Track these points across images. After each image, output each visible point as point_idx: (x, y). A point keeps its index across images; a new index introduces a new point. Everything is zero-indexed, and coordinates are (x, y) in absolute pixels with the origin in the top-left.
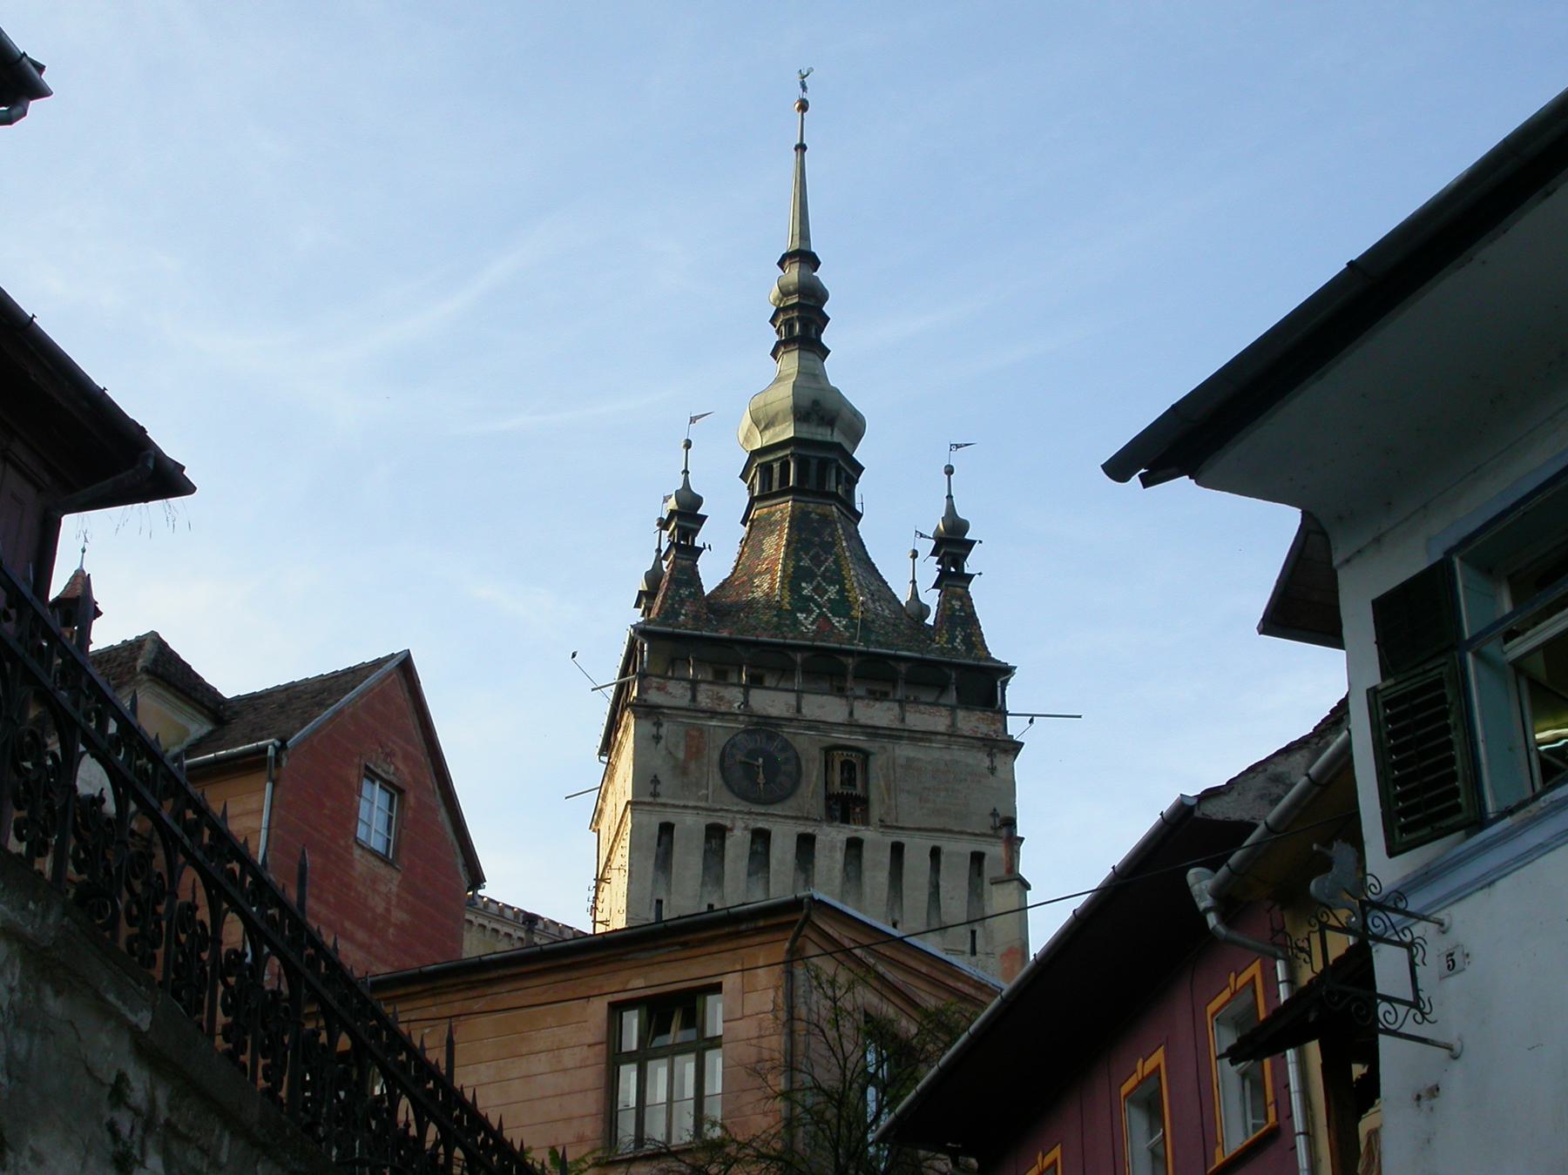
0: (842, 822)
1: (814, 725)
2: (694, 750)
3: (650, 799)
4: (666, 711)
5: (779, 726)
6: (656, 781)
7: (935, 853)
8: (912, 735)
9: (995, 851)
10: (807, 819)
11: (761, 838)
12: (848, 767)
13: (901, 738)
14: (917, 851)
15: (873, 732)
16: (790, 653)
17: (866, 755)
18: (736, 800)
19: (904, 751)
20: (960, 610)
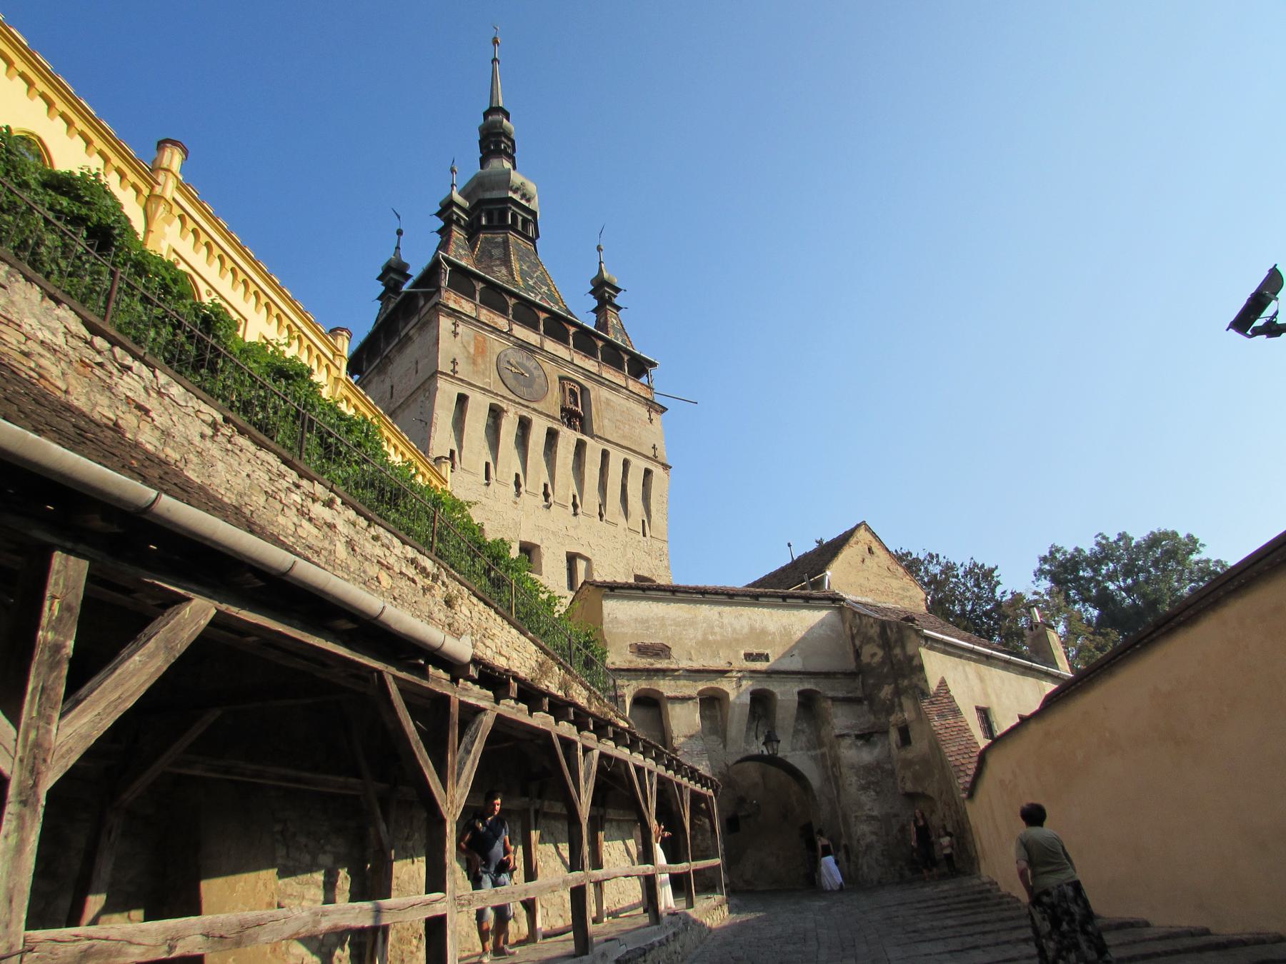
1: (554, 358)
3: (452, 374)
5: (534, 352)
6: (454, 362)
7: (626, 463)
8: (610, 384)
9: (657, 471)
10: (554, 418)
11: (524, 425)
12: (572, 393)
13: (603, 384)
14: (616, 458)
15: (588, 374)
16: (536, 311)
17: (583, 389)
18: (508, 391)
19: (604, 393)
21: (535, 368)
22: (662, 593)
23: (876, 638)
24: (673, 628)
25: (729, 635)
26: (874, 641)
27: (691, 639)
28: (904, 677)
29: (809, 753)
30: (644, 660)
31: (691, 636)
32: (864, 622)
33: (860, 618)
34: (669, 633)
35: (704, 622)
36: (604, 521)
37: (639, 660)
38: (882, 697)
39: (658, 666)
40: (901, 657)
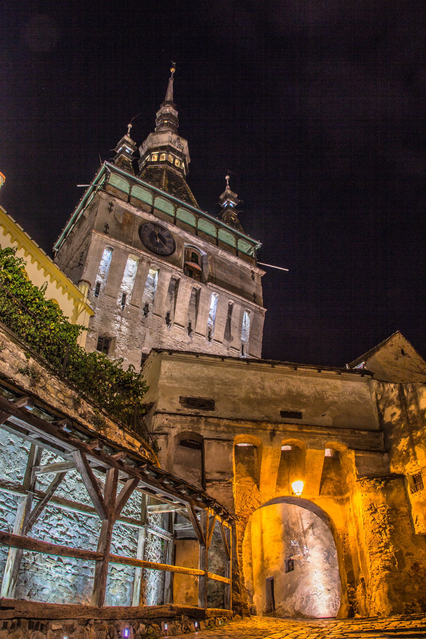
0: (189, 277)
2: (127, 221)
4: (117, 199)
6: (107, 226)
20: (235, 220)
21: (167, 236)
22: (213, 359)
23: (396, 400)
24: (220, 386)
25: (269, 395)
26: (394, 403)
27: (235, 396)
28: (418, 429)
29: (336, 497)
30: (190, 410)
31: (235, 394)
32: (387, 389)
33: (383, 386)
34: (216, 390)
35: (247, 384)
36: (212, 340)
37: (186, 409)
38: (400, 450)
39: (204, 415)
40: (415, 412)
